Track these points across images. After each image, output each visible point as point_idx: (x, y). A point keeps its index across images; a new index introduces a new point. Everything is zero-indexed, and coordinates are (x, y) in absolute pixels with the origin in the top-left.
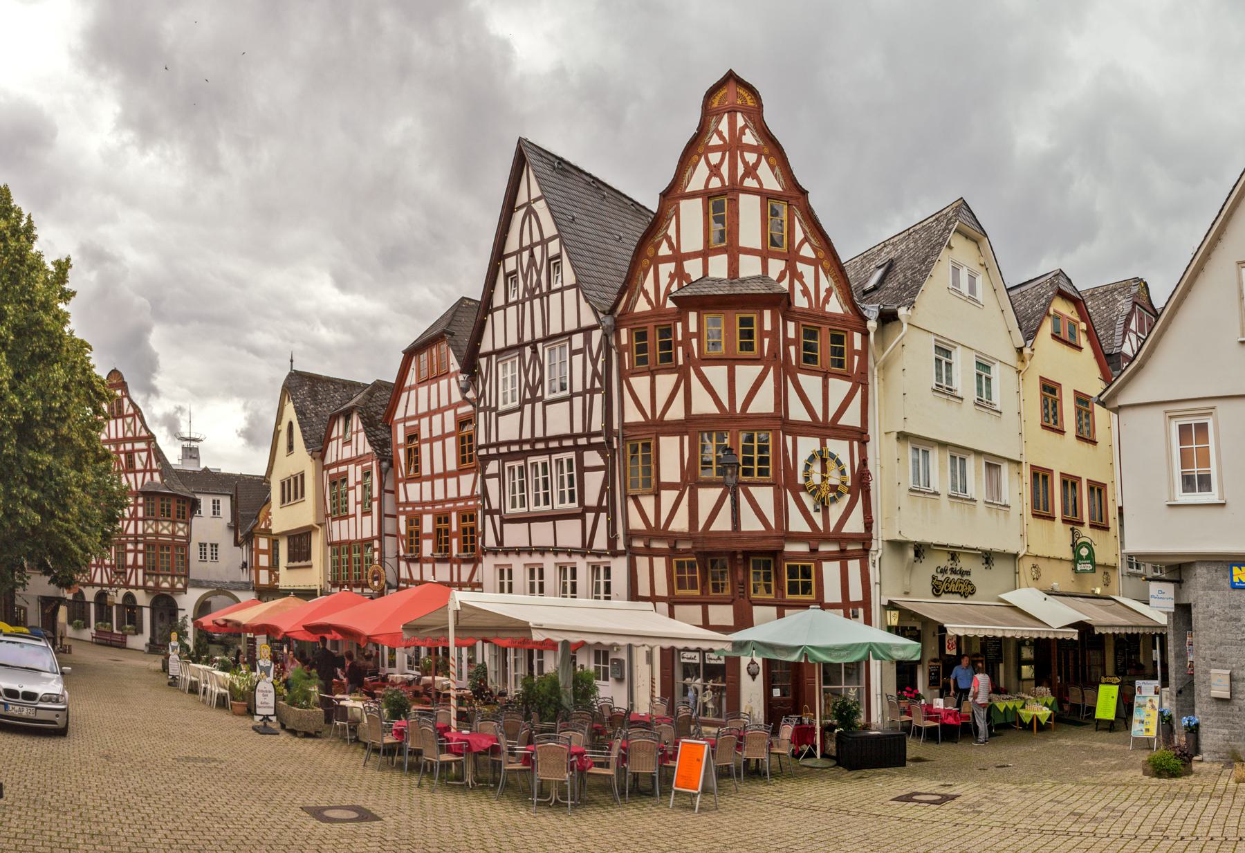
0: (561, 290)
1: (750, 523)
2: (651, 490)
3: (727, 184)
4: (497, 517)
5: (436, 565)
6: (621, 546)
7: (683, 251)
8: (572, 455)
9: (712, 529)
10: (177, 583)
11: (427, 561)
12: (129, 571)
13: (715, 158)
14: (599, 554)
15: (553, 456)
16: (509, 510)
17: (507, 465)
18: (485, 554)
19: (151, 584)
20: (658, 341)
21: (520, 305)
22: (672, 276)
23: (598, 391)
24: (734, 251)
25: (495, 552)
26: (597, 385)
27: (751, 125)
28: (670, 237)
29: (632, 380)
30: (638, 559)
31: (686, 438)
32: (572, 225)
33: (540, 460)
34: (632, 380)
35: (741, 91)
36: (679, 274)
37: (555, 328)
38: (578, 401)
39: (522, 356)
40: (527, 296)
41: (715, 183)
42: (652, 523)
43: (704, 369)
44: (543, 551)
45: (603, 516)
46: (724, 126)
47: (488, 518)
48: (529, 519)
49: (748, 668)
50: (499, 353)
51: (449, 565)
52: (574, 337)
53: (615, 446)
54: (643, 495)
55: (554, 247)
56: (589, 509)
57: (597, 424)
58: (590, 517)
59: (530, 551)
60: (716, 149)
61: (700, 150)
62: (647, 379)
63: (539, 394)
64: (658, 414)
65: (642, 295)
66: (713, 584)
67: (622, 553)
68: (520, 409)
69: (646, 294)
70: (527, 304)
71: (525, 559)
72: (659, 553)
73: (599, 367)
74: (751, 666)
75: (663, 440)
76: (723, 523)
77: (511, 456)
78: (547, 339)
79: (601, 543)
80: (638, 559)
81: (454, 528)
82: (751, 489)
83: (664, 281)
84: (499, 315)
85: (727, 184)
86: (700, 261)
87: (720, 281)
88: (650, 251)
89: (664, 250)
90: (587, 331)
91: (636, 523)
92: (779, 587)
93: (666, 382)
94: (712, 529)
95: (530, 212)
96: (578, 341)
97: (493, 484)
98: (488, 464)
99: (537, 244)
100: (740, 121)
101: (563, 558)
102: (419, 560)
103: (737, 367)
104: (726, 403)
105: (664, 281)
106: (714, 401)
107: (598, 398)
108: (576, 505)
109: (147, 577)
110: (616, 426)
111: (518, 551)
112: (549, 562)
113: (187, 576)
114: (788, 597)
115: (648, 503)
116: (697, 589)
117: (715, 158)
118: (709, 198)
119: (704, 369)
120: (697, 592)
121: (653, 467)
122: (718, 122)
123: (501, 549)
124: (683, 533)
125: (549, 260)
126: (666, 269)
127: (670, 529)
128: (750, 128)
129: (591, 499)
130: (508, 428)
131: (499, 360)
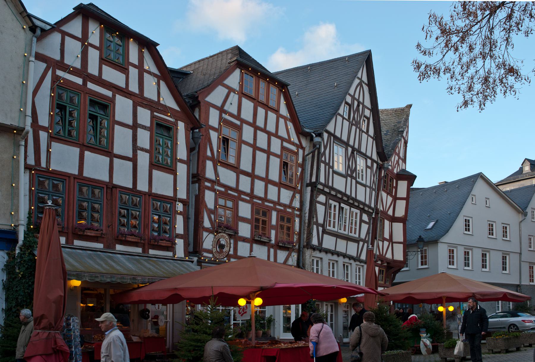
4: (321, 229)
5: (255, 246)
17: (331, 202)
44: (339, 254)
45: (366, 244)
47: (315, 227)
50: (336, 137)
58: (361, 243)
90: (373, 161)
101: (347, 260)
111: (327, 251)
123: (320, 249)
124: (390, 259)
129: (363, 236)
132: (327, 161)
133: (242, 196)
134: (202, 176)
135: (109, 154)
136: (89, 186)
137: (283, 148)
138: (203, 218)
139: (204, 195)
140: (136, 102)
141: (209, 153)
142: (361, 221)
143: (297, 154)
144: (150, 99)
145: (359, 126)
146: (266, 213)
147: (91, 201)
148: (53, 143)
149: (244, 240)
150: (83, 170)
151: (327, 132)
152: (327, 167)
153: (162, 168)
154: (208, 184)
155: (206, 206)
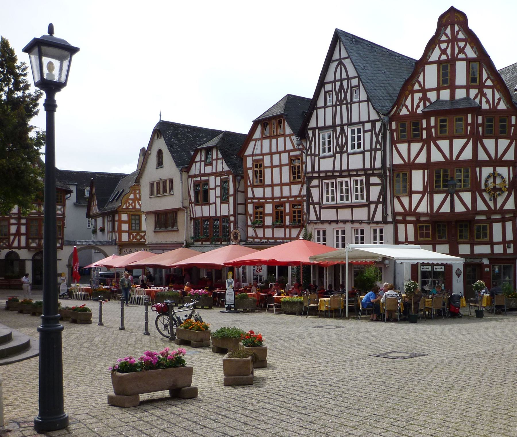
0: (359, 102)
1: (459, 208)
2: (406, 194)
3: (450, 58)
4: (317, 207)
6: (390, 219)
7: (427, 87)
8: (363, 178)
9: (440, 211)
10: (31, 243)
11: (287, 227)
12: (12, 237)
13: (444, 46)
14: (377, 223)
15: (352, 178)
16: (325, 202)
17: (324, 181)
18: (309, 223)
19: (34, 245)
20: (412, 128)
21: (334, 107)
22: (420, 99)
23: (379, 149)
24: (453, 88)
25: (315, 222)
26: (378, 146)
27: (462, 29)
28: (420, 81)
29: (398, 145)
30: (399, 225)
31: (426, 171)
32: (364, 71)
33: (344, 180)
34: (398, 145)
35: (457, 15)
36: (424, 98)
37: (355, 119)
38: (367, 155)
39: (335, 131)
40: (338, 103)
41: (444, 57)
42: (408, 209)
43: (438, 142)
44: (345, 222)
45: (380, 206)
46: (448, 31)
47: (311, 207)
48: (337, 207)
49: (456, 272)
50: (320, 129)
51: (283, 229)
52: (366, 125)
53: (388, 174)
54: (402, 196)
55: (354, 82)
56: (373, 203)
57: (378, 164)
58: (373, 207)
59: (337, 222)
60: (444, 42)
61: (436, 42)
62: (406, 145)
63: (345, 149)
64: (411, 160)
65: (404, 107)
66: (438, 235)
67: (391, 223)
68: (334, 156)
69: (407, 107)
70: (338, 108)
71: (334, 225)
72: (410, 222)
73: (380, 139)
74: (457, 271)
75: (413, 172)
76: (446, 209)
77: (327, 177)
78: (350, 124)
79: (379, 217)
80: (399, 225)
81: (287, 210)
82: (460, 194)
83: (416, 101)
84: (321, 112)
85: (450, 58)
86: (435, 93)
87: (446, 102)
88: (409, 88)
89: (417, 87)
91: (398, 208)
92: (472, 235)
93: (416, 147)
94: (440, 211)
95: (341, 63)
96: (368, 126)
97: (315, 192)
98: (312, 181)
99: (345, 79)
100: (457, 28)
101: (356, 225)
102: (263, 227)
103: (454, 140)
104: (448, 156)
105: (416, 101)
106: (442, 155)
107: (379, 153)
108: (365, 200)
109: (30, 241)
110: (388, 165)
111: (330, 222)
112: (348, 227)
113: (62, 239)
114: (476, 240)
115: (405, 200)
116: (430, 237)
117: (444, 46)
118: (440, 64)
119: (438, 142)
120: (430, 239)
121: (408, 184)
122: (446, 29)
125: (351, 88)
126: (417, 96)
127: (417, 211)
128: (461, 31)
129: (374, 197)
130: (326, 165)
131: (320, 132)
132: (313, 152)
133: (268, 201)
137: (290, 157)
141: (249, 184)
142: (368, 185)
143: (301, 155)
145: (345, 102)
146: (283, 205)
149: (268, 227)
151: (310, 129)
152: (313, 157)
155: (249, 213)
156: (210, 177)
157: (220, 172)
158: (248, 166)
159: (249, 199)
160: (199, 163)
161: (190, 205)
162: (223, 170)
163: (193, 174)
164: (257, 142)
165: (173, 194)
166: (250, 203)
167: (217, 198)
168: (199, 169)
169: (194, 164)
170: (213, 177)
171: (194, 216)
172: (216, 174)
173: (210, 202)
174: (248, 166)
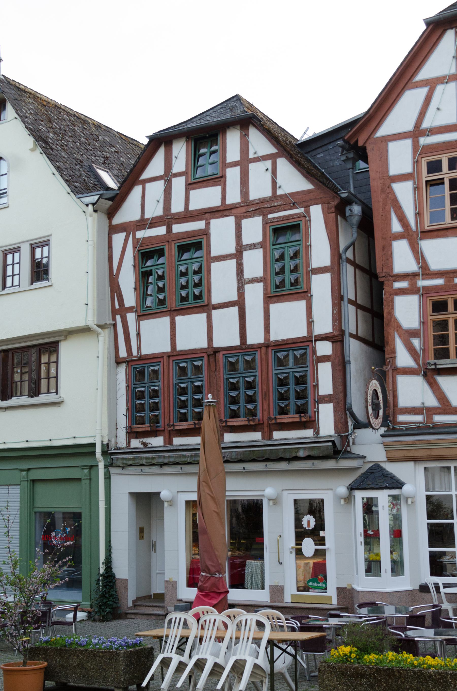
134: (384, 275)
135: (206, 308)
136: (187, 360)
138: (394, 351)
139: (393, 308)
140: (239, 215)
144: (260, 199)
147: (190, 380)
148: (141, 322)
150: (245, 331)
153: (286, 297)
154: (398, 285)
155: (399, 326)
156: (214, 222)
157: (262, 201)
158: (393, 170)
159: (395, 281)
160: (161, 185)
161: (114, 319)
162: (279, 192)
163: (137, 216)
164: (439, 88)
165: (51, 286)
166: (402, 292)
167: (248, 288)
168: (162, 200)
169: (137, 191)
170: (230, 221)
171: (135, 353)
172: (243, 210)
173: (215, 300)
174: (393, 170)
